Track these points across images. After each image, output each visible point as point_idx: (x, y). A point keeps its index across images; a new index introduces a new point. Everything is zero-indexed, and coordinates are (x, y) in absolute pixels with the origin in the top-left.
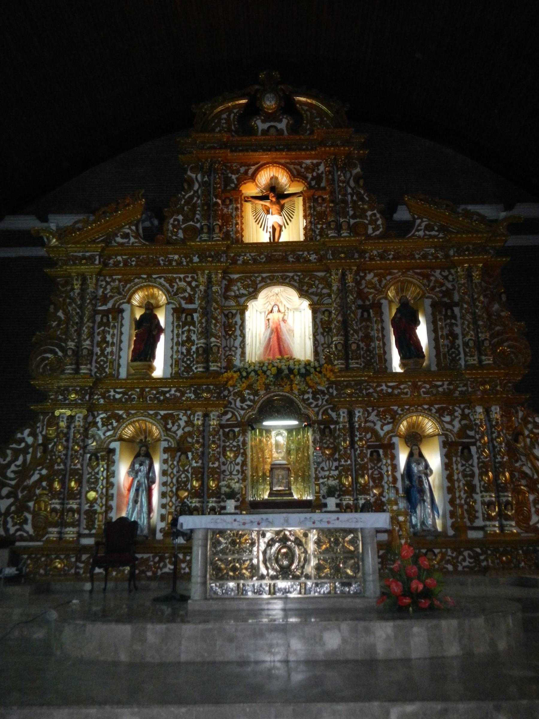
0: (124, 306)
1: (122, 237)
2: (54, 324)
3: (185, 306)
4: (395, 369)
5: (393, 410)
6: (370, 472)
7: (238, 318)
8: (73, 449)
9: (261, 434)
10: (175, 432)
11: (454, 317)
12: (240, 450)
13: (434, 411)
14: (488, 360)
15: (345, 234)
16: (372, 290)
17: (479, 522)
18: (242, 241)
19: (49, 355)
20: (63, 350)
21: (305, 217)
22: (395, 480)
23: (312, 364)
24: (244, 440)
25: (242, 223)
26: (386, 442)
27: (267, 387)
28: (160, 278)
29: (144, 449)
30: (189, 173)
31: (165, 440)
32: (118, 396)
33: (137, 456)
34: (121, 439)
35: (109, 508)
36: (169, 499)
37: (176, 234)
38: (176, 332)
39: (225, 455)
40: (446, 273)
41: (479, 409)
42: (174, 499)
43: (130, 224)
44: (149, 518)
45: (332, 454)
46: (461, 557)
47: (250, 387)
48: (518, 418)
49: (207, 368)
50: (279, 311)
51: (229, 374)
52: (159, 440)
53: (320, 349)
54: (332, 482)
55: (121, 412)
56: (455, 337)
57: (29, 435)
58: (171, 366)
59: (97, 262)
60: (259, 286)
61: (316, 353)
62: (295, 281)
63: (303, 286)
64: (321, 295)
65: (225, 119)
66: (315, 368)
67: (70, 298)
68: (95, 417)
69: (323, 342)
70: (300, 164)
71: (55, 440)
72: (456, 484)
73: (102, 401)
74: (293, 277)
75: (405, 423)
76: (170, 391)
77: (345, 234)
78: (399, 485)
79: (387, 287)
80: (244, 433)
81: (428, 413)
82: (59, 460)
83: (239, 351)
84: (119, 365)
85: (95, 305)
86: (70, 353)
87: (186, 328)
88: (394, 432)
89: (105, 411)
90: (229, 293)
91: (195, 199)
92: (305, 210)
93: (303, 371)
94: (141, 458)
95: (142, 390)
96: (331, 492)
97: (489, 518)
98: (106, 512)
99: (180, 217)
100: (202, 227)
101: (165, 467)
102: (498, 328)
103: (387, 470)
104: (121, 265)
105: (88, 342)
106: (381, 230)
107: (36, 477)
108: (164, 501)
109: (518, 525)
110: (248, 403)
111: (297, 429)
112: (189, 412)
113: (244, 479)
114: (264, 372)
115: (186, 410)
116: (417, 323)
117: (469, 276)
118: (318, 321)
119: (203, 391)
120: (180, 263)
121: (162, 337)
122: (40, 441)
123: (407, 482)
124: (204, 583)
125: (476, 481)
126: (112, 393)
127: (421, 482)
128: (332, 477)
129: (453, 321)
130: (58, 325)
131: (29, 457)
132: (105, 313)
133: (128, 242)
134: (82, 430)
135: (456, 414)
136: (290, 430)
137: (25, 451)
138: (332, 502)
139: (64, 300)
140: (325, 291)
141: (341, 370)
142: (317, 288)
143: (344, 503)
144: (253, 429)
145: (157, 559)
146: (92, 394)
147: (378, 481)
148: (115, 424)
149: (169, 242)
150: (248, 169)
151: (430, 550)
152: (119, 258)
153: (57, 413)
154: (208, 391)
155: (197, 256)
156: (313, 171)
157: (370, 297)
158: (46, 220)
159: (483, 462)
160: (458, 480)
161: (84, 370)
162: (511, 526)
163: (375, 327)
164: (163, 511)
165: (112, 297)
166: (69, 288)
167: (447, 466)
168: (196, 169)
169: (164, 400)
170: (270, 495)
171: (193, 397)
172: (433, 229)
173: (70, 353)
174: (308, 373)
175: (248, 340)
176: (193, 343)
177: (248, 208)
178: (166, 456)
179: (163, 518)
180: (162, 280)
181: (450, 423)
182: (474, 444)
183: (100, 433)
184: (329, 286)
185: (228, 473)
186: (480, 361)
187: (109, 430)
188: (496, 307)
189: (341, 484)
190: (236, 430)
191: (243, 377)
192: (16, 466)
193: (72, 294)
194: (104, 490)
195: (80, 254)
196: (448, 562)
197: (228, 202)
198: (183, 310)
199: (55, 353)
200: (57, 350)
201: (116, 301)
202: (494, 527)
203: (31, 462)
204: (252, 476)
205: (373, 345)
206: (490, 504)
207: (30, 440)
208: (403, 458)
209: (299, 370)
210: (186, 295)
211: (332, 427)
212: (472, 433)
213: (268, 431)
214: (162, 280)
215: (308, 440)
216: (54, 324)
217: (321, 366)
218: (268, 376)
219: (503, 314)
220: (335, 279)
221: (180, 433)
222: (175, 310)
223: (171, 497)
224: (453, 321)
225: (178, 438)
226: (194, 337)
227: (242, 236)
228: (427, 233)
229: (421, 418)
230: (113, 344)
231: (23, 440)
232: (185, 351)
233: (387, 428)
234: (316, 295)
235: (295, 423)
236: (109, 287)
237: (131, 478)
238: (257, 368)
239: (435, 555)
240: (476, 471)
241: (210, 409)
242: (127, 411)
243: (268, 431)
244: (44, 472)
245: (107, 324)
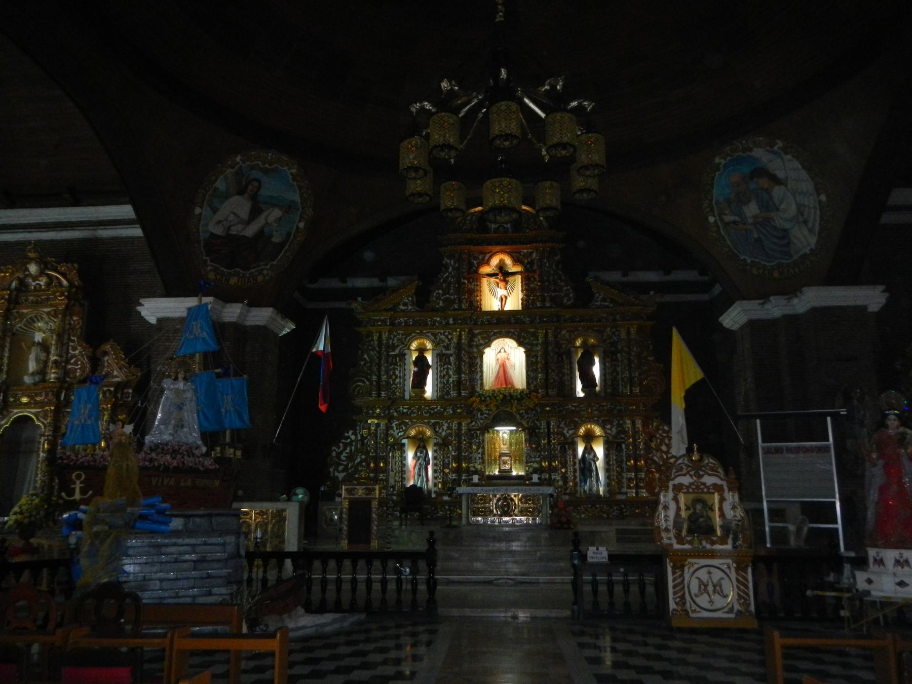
0: (406, 351)
1: (403, 306)
2: (362, 363)
3: (444, 352)
4: (579, 393)
5: (575, 421)
6: (559, 459)
7: (478, 360)
8: (380, 443)
9: (493, 433)
10: (441, 433)
11: (617, 360)
12: (481, 445)
13: (600, 421)
14: (637, 390)
15: (548, 304)
16: (564, 342)
17: (624, 490)
18: (481, 308)
19: (361, 384)
20: (368, 380)
21: (522, 291)
22: (575, 464)
23: (525, 392)
24: (483, 439)
25: (481, 296)
26: (570, 441)
27: (497, 407)
28: (428, 333)
29: (422, 443)
30: (445, 259)
31: (435, 438)
32: (405, 411)
33: (418, 448)
34: (408, 437)
35: (403, 479)
36: (438, 474)
37: (438, 304)
38: (439, 369)
39: (471, 448)
40: (614, 330)
41: (628, 422)
42: (442, 474)
43: (408, 296)
44: (427, 485)
45: (537, 448)
46: (612, 510)
47: (487, 406)
48: (652, 426)
49: (460, 394)
50: (505, 351)
51: (474, 399)
52: (429, 438)
53: (530, 381)
54: (536, 465)
55: (407, 421)
56: (618, 374)
57: (352, 435)
58: (437, 391)
59: (388, 324)
60: (492, 339)
61: (528, 383)
62: (515, 335)
63: (520, 339)
64: (532, 345)
65: (469, 220)
66: (526, 394)
67: (372, 346)
68: (391, 424)
69: (532, 376)
70: (519, 253)
71: (369, 437)
72: (612, 467)
73: (395, 414)
74: (514, 332)
75: (583, 428)
76: (437, 407)
77: (548, 304)
78: (577, 466)
79: (575, 339)
80: (483, 434)
81: (597, 423)
82: (372, 451)
83: (479, 382)
84: (404, 391)
85: (388, 352)
86: (374, 383)
87: (446, 366)
88: (575, 435)
89: (398, 420)
90: (472, 343)
91: (450, 278)
92: (522, 286)
93: (519, 396)
94: (420, 449)
95: (420, 407)
96: (535, 471)
97: (629, 488)
98: (402, 481)
99: (441, 292)
100: (455, 299)
101: (436, 455)
102: (645, 368)
103: (570, 459)
104: (403, 324)
105: (385, 377)
106: (572, 301)
108: (436, 475)
109: (647, 491)
110: (485, 415)
111: (516, 431)
112: (449, 421)
113: (483, 462)
114: (495, 397)
115: (447, 420)
116: (593, 363)
117: (628, 333)
118: (529, 362)
119: (458, 408)
120: (440, 323)
121: (430, 371)
122: (359, 438)
123: (582, 465)
124: (468, 518)
125: (624, 466)
126: (401, 409)
127: (591, 466)
128: (536, 462)
129: (617, 363)
130: (365, 364)
131: (353, 448)
133: (407, 309)
134: (385, 432)
135: (615, 424)
136: (511, 431)
137: (350, 444)
138: (535, 478)
139: (368, 347)
140: (535, 342)
141: (543, 397)
142: (529, 339)
143: (543, 477)
144: (488, 432)
145: (433, 508)
146: (389, 409)
147: (564, 464)
148: (404, 428)
149: (434, 310)
150: (485, 257)
151: (593, 505)
152: (402, 319)
153: (369, 421)
154: (461, 408)
155: (452, 319)
156: (528, 258)
157: (564, 346)
158: (346, 282)
159: (629, 455)
160: (613, 464)
161: (383, 394)
162: (643, 492)
163: (566, 367)
164: (436, 481)
165: (398, 346)
166: (370, 338)
167: (607, 456)
168: (450, 257)
169: (433, 413)
170: (499, 472)
171: (451, 412)
172: (606, 301)
173: (374, 383)
174: (522, 398)
175: (485, 369)
176: (450, 377)
177: (485, 281)
178: (435, 448)
179: (435, 485)
180: (429, 334)
181: (610, 429)
182: (624, 443)
183: (395, 434)
184: (537, 338)
185: (473, 459)
186: (631, 391)
187: (400, 432)
188: (645, 354)
189: (541, 465)
190: (478, 432)
191: (482, 401)
192: (346, 453)
193: (372, 343)
194: (400, 469)
195: (378, 318)
196: (604, 512)
197: (471, 280)
198: (444, 355)
199: (365, 383)
200: (365, 380)
201: (401, 349)
202: (633, 493)
203: (355, 450)
204: (488, 460)
205: (564, 378)
206: (630, 480)
207: (353, 437)
208: (580, 449)
209: (517, 396)
210: (446, 344)
211: (537, 431)
212: (623, 436)
213: (498, 431)
214: (429, 334)
215: (522, 438)
216: (362, 363)
217: (530, 392)
218: (497, 400)
219: (649, 358)
220: (541, 334)
221: (444, 434)
222: (438, 355)
223: (440, 473)
224: (617, 363)
225: (443, 437)
226: (451, 373)
227: (481, 304)
228: (603, 303)
229: (593, 426)
230: (400, 377)
231: (349, 437)
232: (445, 382)
233: (571, 432)
234: (529, 345)
235: (514, 428)
236: (395, 339)
237: (415, 461)
238: (491, 394)
239: (596, 508)
240: (625, 459)
241: (462, 420)
242: (411, 420)
243: (498, 431)
244: (363, 457)
245: (396, 364)
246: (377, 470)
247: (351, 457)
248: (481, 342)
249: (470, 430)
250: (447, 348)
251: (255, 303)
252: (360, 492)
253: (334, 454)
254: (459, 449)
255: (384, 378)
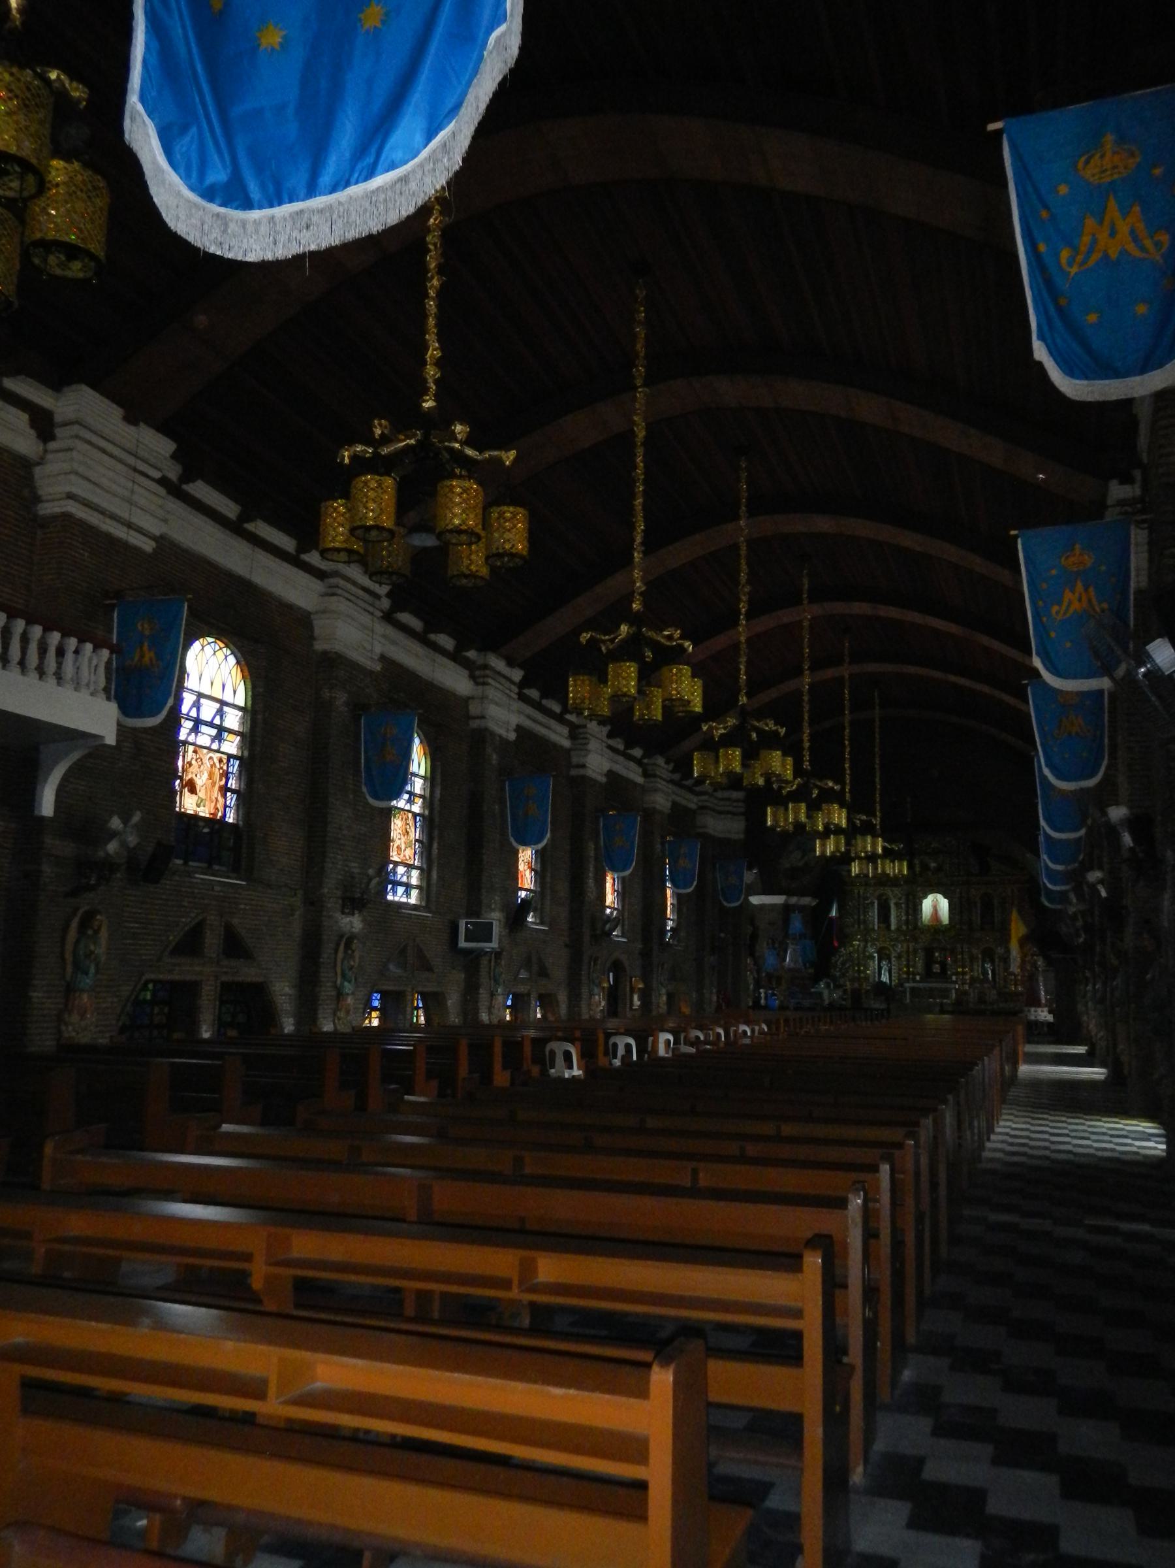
7: (919, 907)
54: (954, 971)
107: (847, 965)
132: (868, 904)
137: (843, 956)
161: (862, 927)
246: (859, 971)
247: (843, 964)
248: (921, 895)
249: (914, 949)
250: (900, 899)
251: (803, 895)
252: (856, 985)
253: (833, 961)
254: (908, 961)
255: (862, 917)
